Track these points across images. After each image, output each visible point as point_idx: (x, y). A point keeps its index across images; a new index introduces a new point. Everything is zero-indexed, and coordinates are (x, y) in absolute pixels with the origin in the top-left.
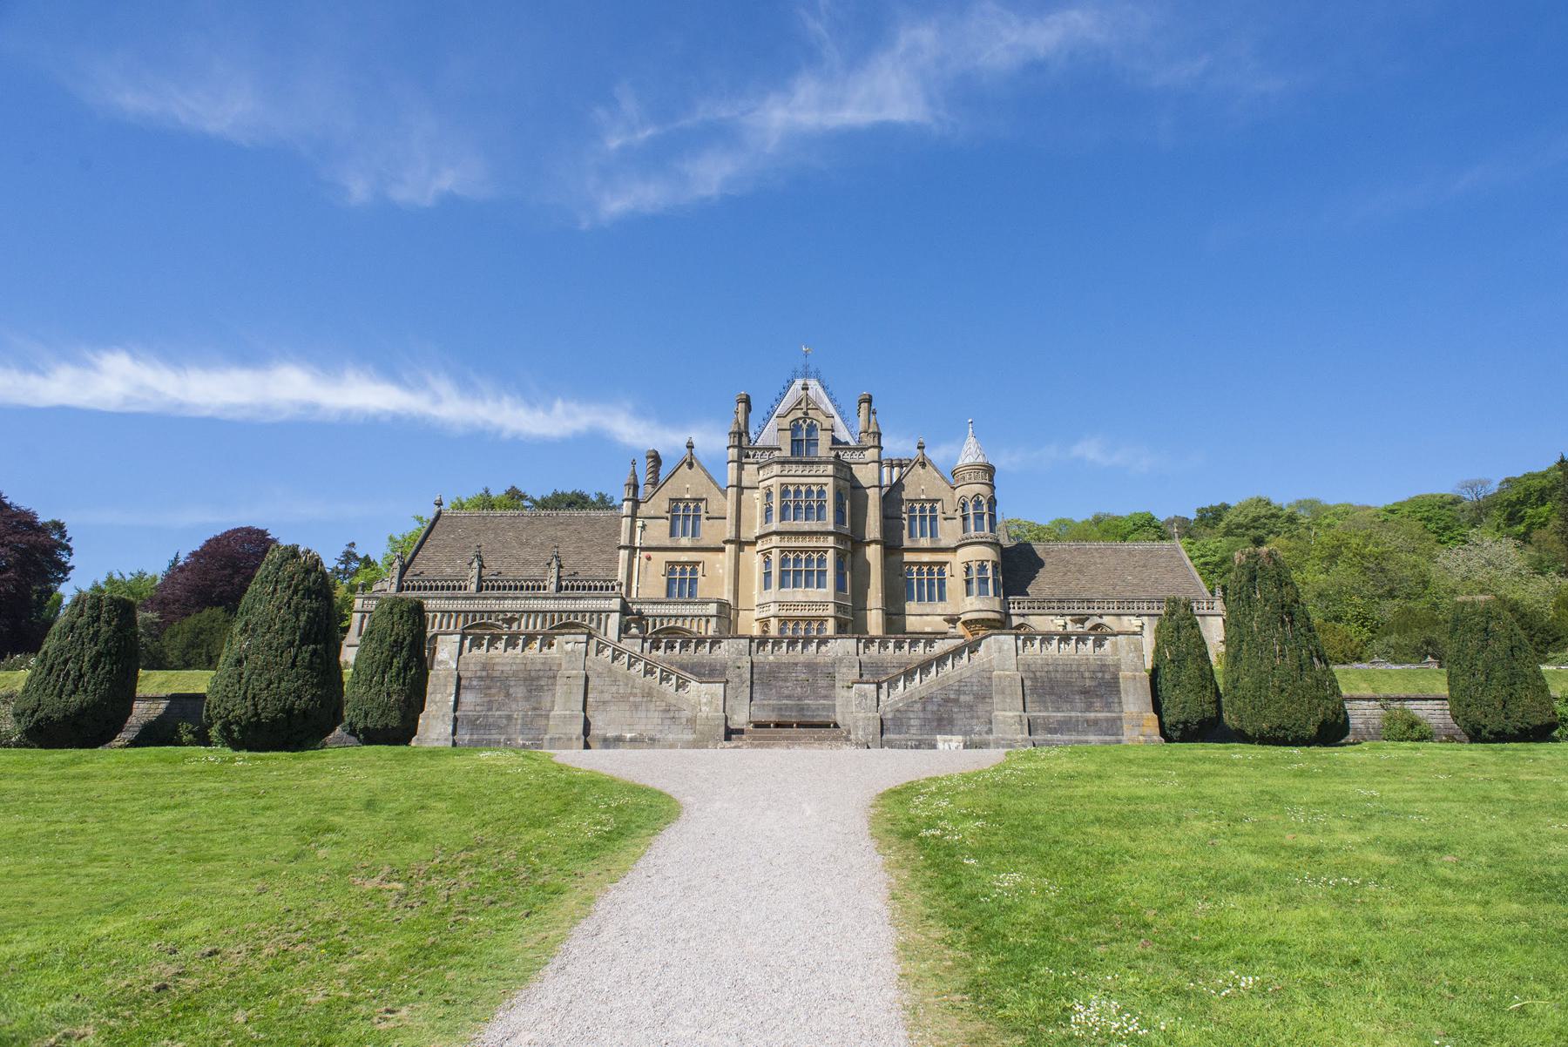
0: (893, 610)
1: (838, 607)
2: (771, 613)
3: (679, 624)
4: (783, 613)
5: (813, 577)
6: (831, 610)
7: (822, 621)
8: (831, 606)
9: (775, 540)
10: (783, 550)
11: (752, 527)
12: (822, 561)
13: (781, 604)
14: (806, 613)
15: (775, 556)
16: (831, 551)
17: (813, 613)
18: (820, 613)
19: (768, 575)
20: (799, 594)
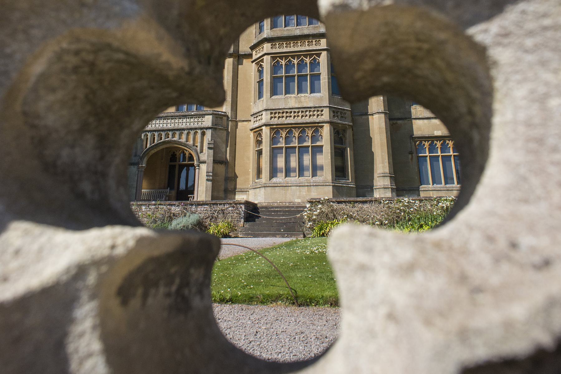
0: (397, 115)
1: (334, 112)
2: (263, 121)
3: (176, 138)
4: (275, 121)
5: (306, 81)
6: (326, 115)
7: (317, 127)
8: (326, 112)
9: (267, 47)
10: (274, 57)
11: (267, 59)
12: (315, 64)
13: (273, 111)
14: (299, 120)
15: (267, 62)
16: (324, 54)
17: (307, 119)
18: (314, 119)
19: (261, 83)
20: (292, 101)
